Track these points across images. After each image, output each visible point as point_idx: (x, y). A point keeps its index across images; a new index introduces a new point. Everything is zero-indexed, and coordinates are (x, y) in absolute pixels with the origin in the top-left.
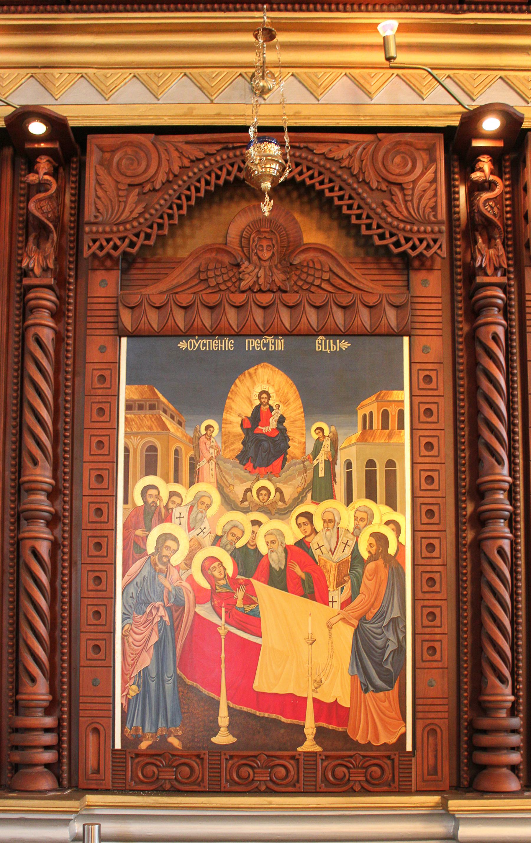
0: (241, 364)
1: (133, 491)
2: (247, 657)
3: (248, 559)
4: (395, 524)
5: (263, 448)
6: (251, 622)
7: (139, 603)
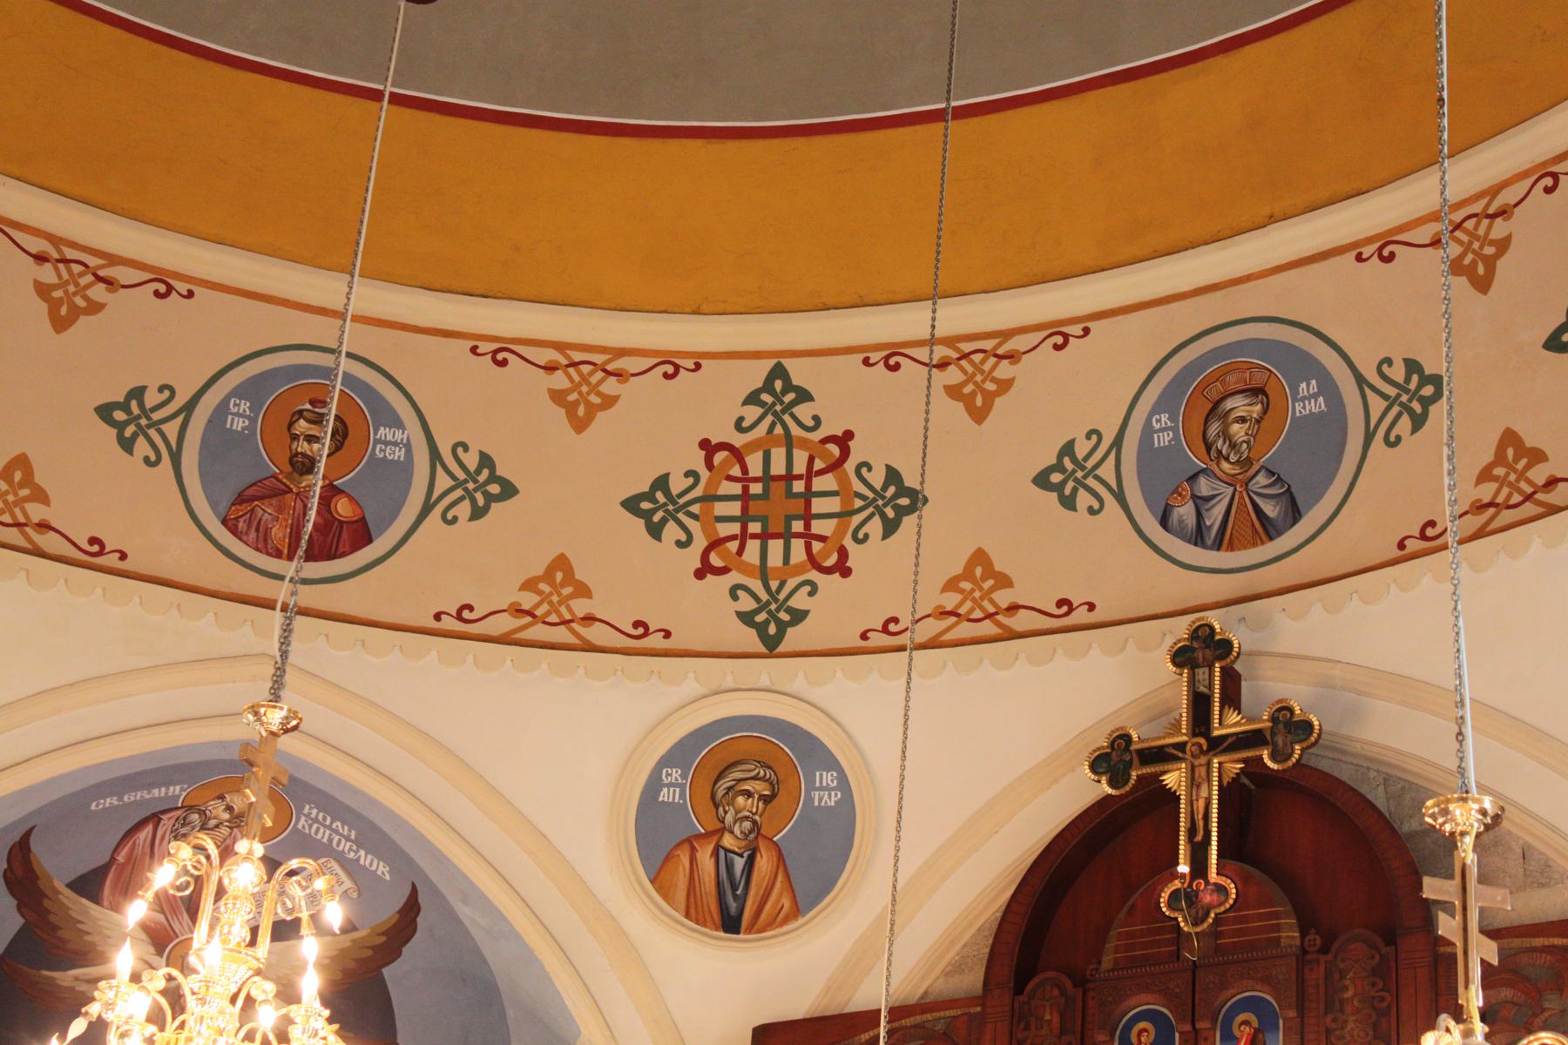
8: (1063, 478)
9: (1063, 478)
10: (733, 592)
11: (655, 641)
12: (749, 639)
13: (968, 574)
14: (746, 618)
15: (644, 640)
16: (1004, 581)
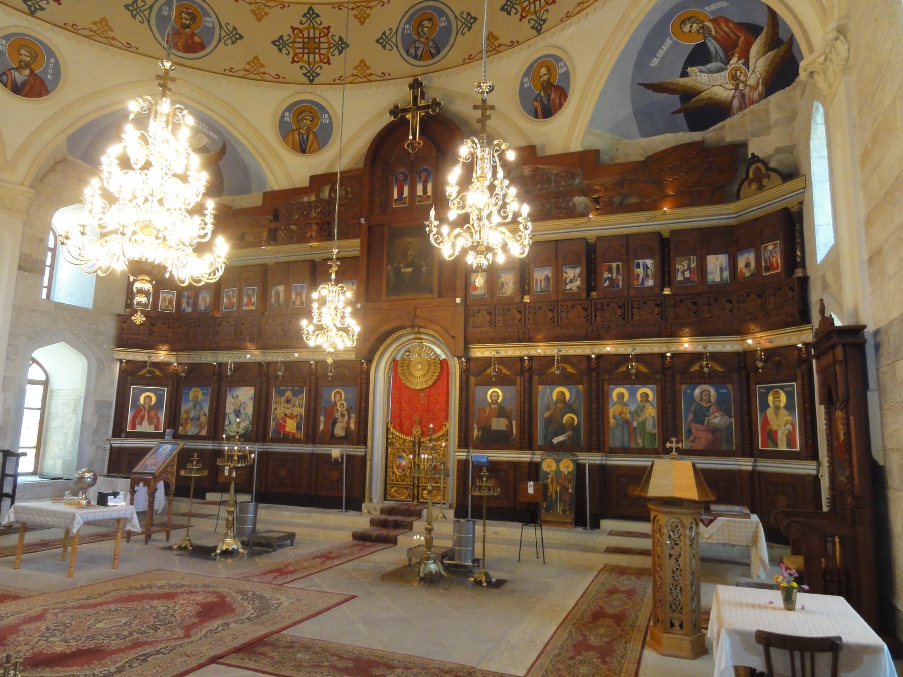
0: (285, 391)
1: (274, 406)
2: (285, 427)
3: (286, 415)
4: (302, 411)
5: (288, 401)
6: (285, 422)
7: (274, 419)
8: (383, 40)
9: (383, 40)
10: (301, 67)
11: (282, 79)
12: (305, 80)
13: (359, 65)
14: (304, 74)
15: (279, 79)
16: (368, 68)
